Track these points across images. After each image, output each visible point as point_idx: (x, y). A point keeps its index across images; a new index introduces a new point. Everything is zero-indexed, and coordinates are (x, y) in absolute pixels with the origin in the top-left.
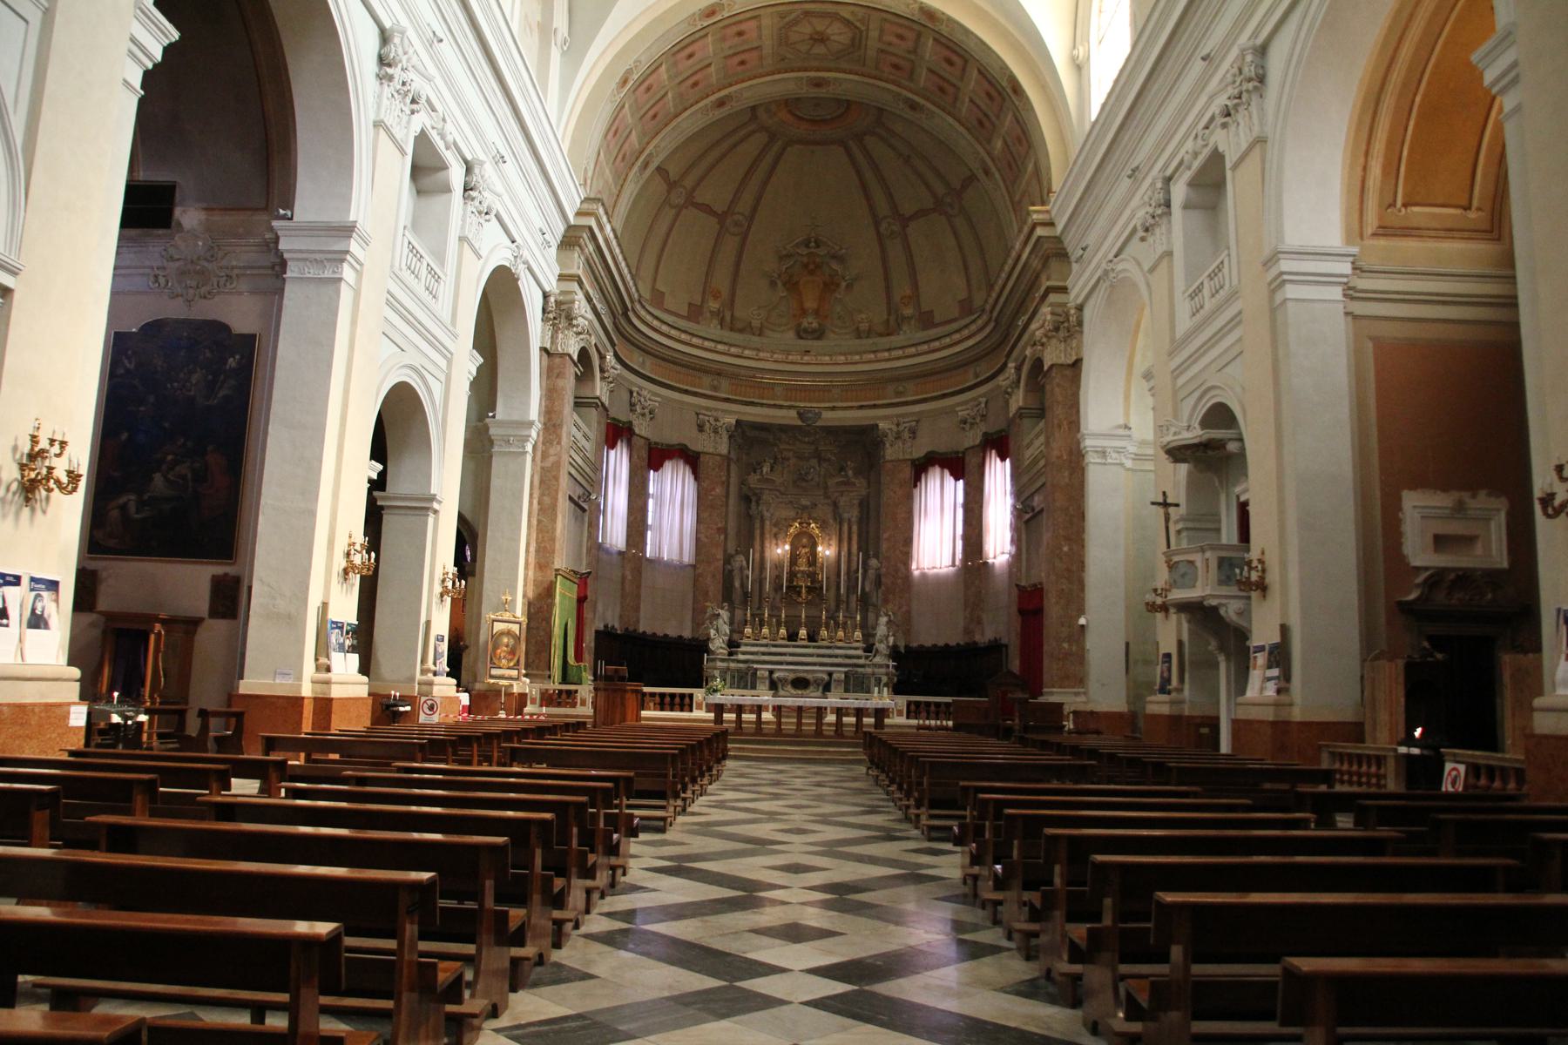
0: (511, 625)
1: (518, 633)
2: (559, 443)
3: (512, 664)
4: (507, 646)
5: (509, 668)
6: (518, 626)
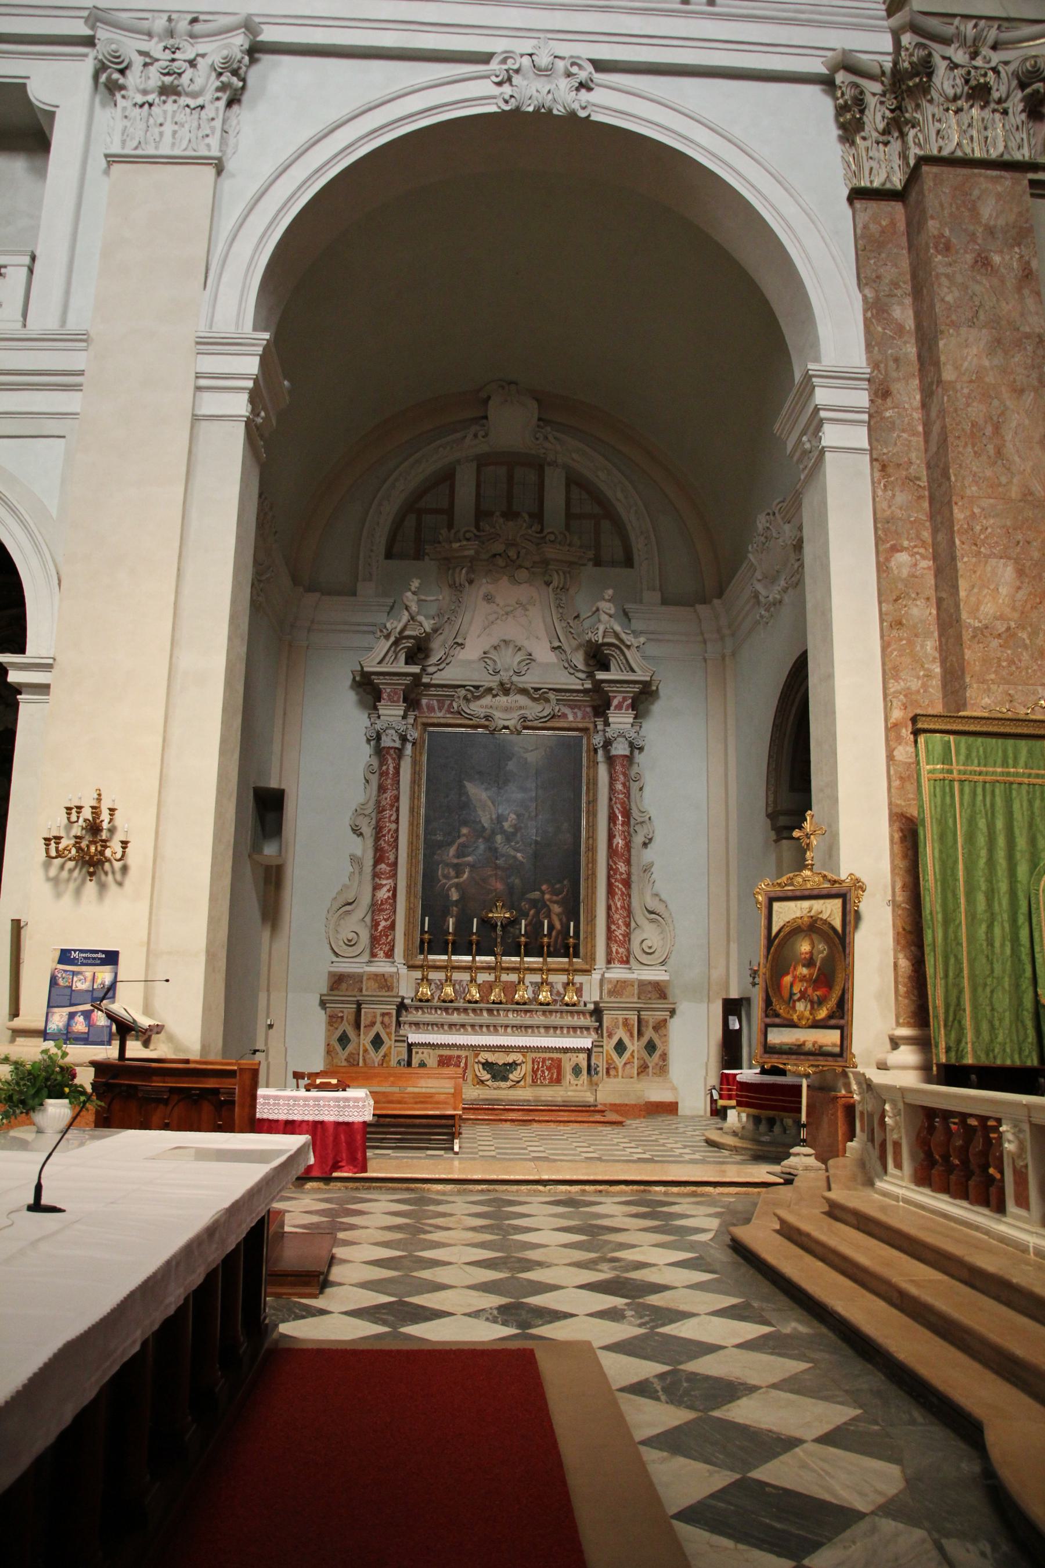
0: (817, 905)
1: (837, 924)
2: (940, 382)
3: (822, 1013)
4: (810, 963)
5: (816, 1025)
6: (837, 903)
